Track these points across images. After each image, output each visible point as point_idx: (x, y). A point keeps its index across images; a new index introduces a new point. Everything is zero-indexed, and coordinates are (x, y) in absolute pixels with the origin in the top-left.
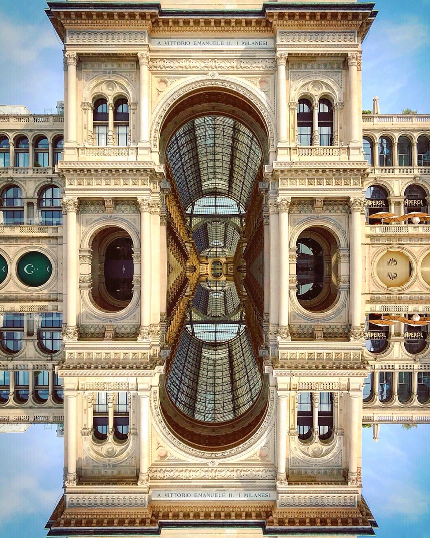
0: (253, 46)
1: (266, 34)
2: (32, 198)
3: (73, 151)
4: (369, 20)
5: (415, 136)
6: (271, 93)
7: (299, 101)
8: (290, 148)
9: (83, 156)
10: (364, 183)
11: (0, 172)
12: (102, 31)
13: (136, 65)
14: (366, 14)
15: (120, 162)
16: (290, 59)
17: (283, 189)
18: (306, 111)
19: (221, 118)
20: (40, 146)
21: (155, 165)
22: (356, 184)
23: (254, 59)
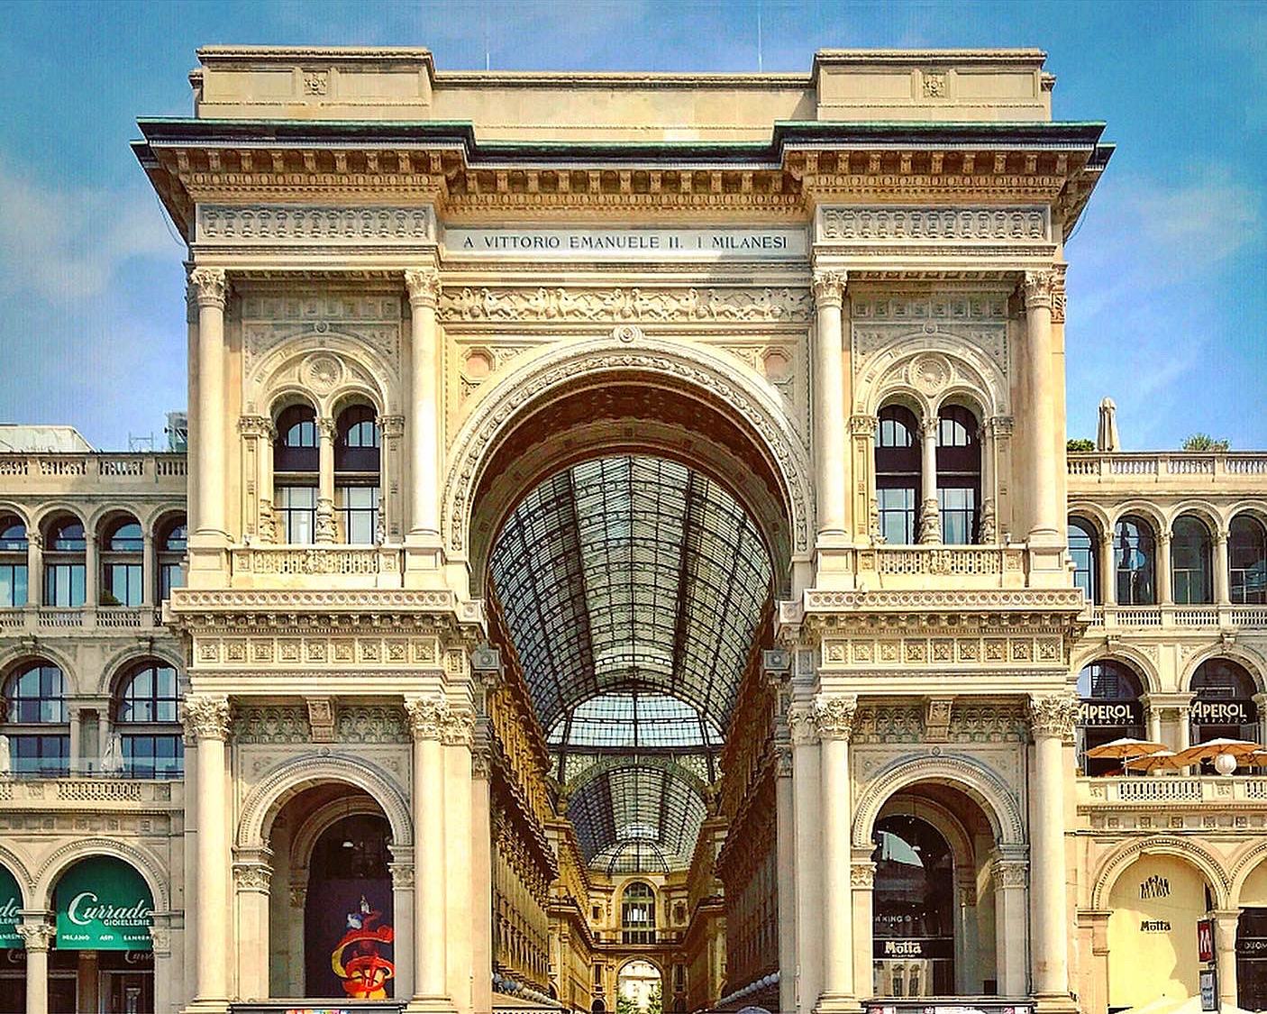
0: (745, 251)
1: (783, 216)
2: (96, 698)
3: (215, 559)
4: (1086, 173)
5: (1222, 516)
6: (798, 388)
7: (879, 413)
8: (855, 552)
9: (244, 574)
10: (1073, 656)
11: (2, 623)
12: (300, 205)
13: (399, 305)
14: (1077, 157)
15: (353, 593)
16: (854, 288)
17: (834, 673)
18: (901, 442)
19: (652, 463)
20: (117, 546)
21: (457, 600)
22: (1048, 656)
23: (746, 289)
